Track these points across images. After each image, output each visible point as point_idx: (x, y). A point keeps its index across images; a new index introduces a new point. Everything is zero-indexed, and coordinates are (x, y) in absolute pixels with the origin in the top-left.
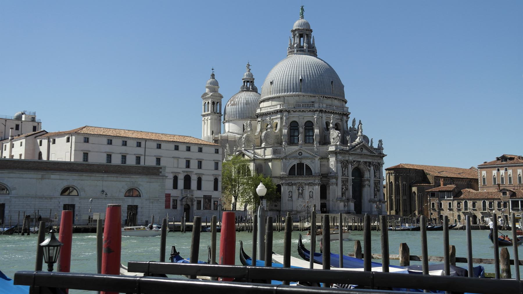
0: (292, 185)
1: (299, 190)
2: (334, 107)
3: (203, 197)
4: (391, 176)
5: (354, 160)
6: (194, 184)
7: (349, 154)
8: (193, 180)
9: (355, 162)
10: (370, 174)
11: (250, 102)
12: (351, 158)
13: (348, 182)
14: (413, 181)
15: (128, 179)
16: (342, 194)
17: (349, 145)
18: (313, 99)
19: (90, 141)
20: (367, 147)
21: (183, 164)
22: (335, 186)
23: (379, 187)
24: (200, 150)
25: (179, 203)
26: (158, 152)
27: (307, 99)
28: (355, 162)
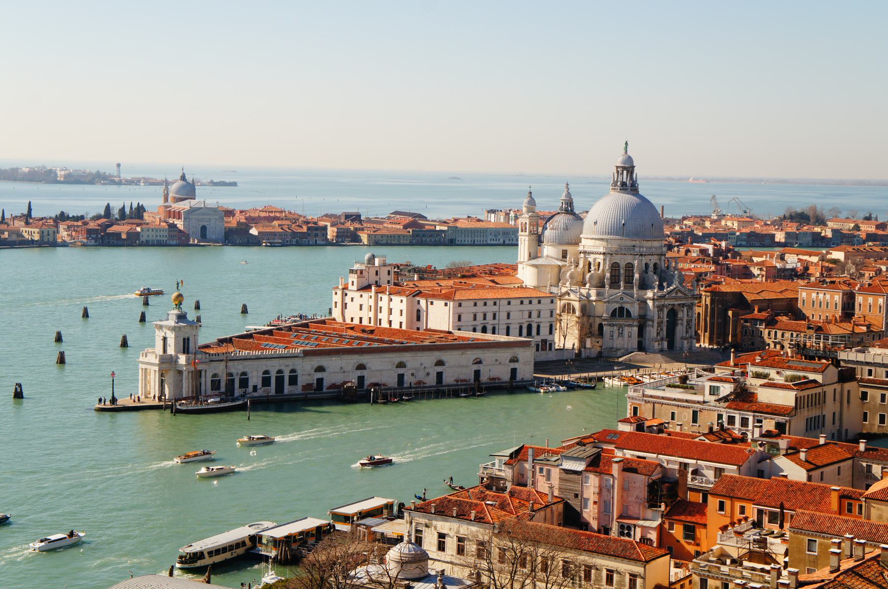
0: (614, 325)
1: (619, 330)
4: (707, 299)
7: (665, 299)
11: (568, 227)
12: (666, 303)
15: (511, 351)
16: (657, 334)
17: (665, 290)
18: (634, 243)
19: (462, 305)
21: (526, 314)
22: (651, 328)
24: (539, 302)
26: (508, 308)
27: (630, 243)
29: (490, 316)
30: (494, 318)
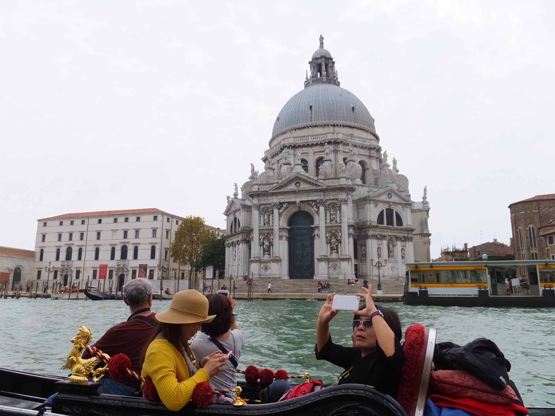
2: (310, 138)
3: (138, 266)
5: (281, 201)
6: (130, 254)
8: (130, 250)
9: (285, 204)
10: (319, 218)
13: (273, 234)
14: (551, 221)
19: (48, 225)
20: (304, 179)
23: (341, 237)
24: (138, 219)
25: (114, 273)
26: (99, 227)
28: (285, 204)
29: (76, 236)
30: (82, 239)
